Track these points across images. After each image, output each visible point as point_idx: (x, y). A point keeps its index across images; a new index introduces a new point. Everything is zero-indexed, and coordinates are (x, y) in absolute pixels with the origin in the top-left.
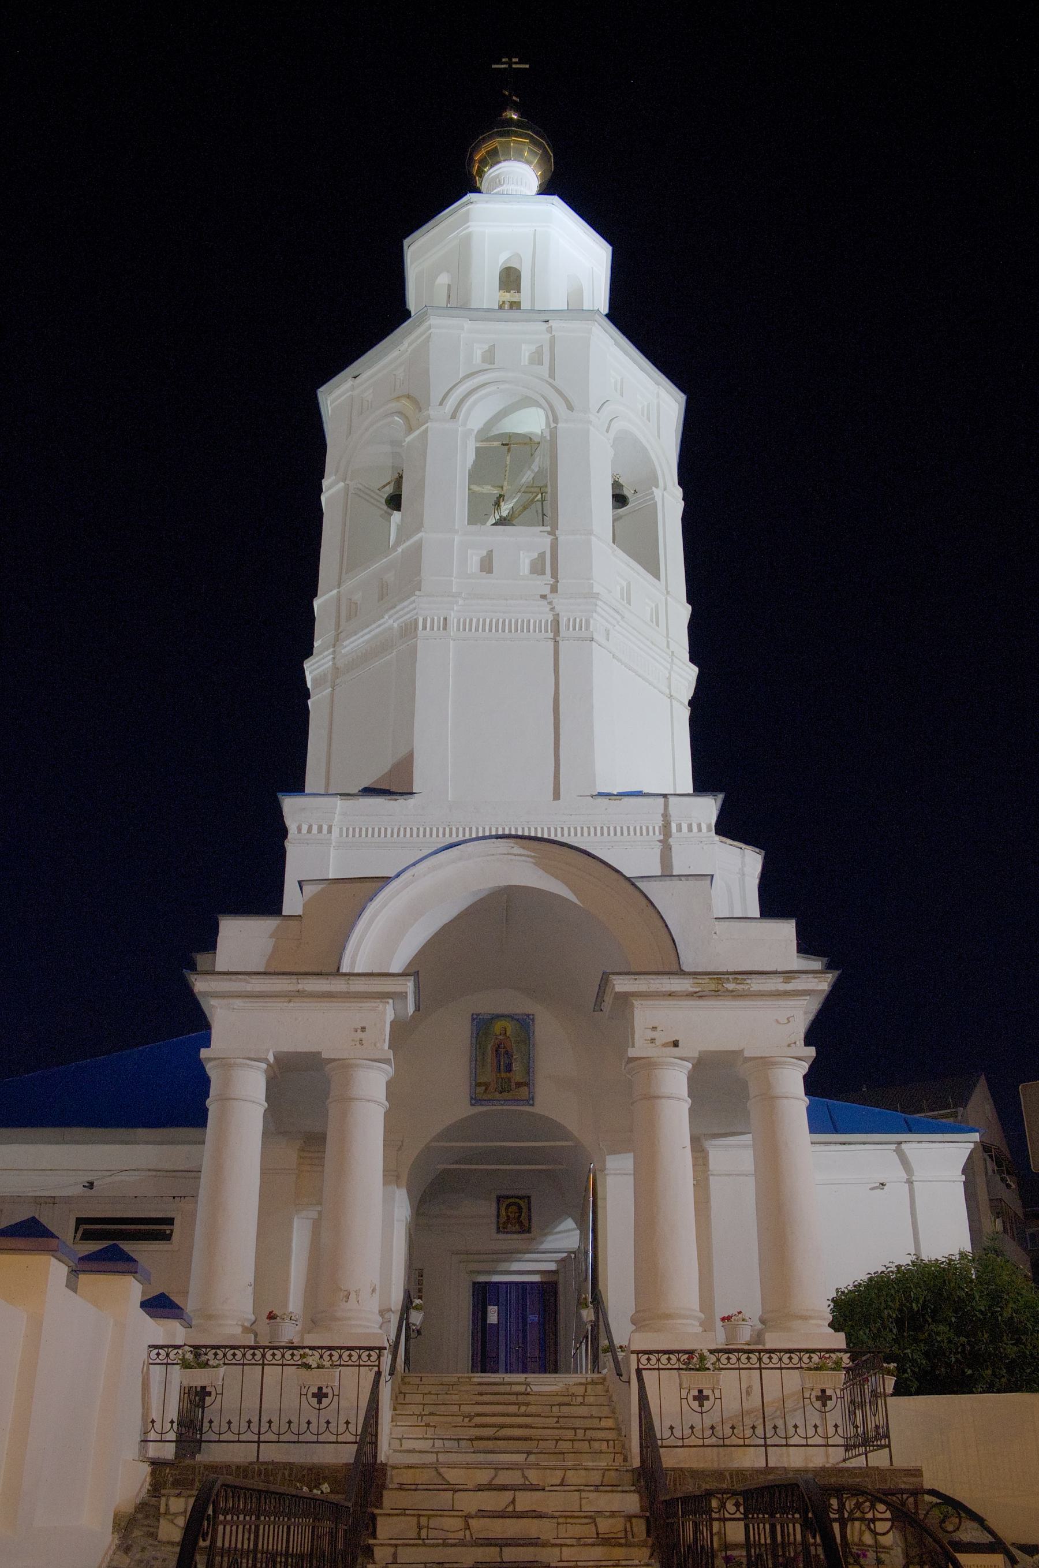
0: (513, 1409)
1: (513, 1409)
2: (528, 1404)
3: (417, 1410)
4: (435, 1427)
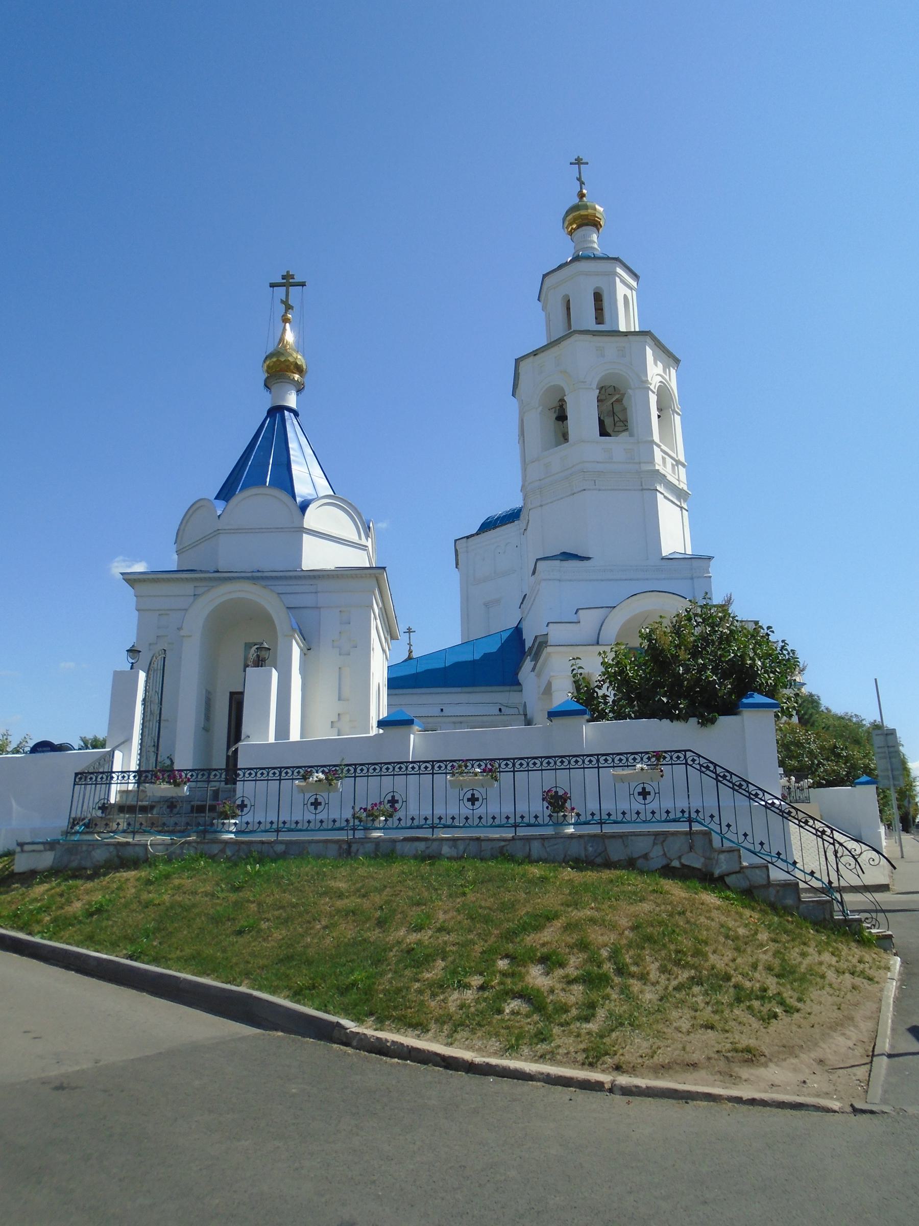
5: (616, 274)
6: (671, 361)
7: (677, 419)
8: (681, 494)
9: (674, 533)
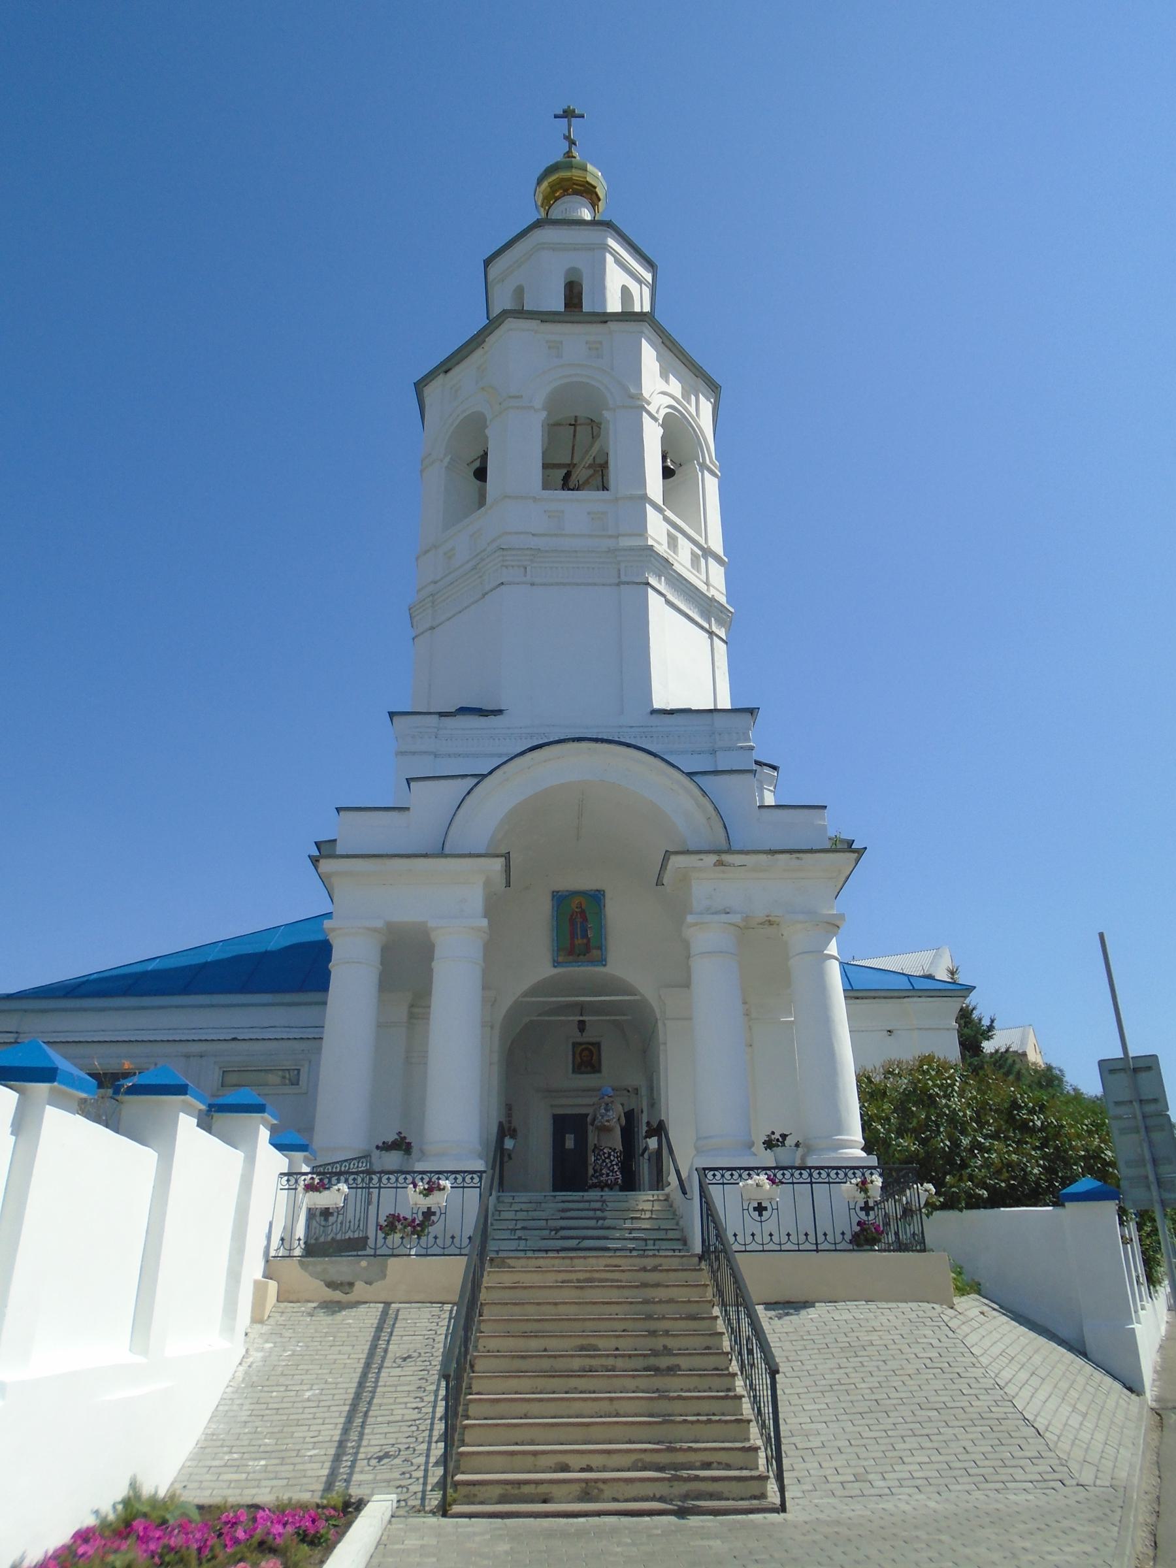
0: (592, 1223)
1: (592, 1223)
2: (604, 1219)
3: (511, 1225)
5: (606, 248)
6: (700, 383)
7: (711, 485)
8: (707, 606)
9: (686, 667)
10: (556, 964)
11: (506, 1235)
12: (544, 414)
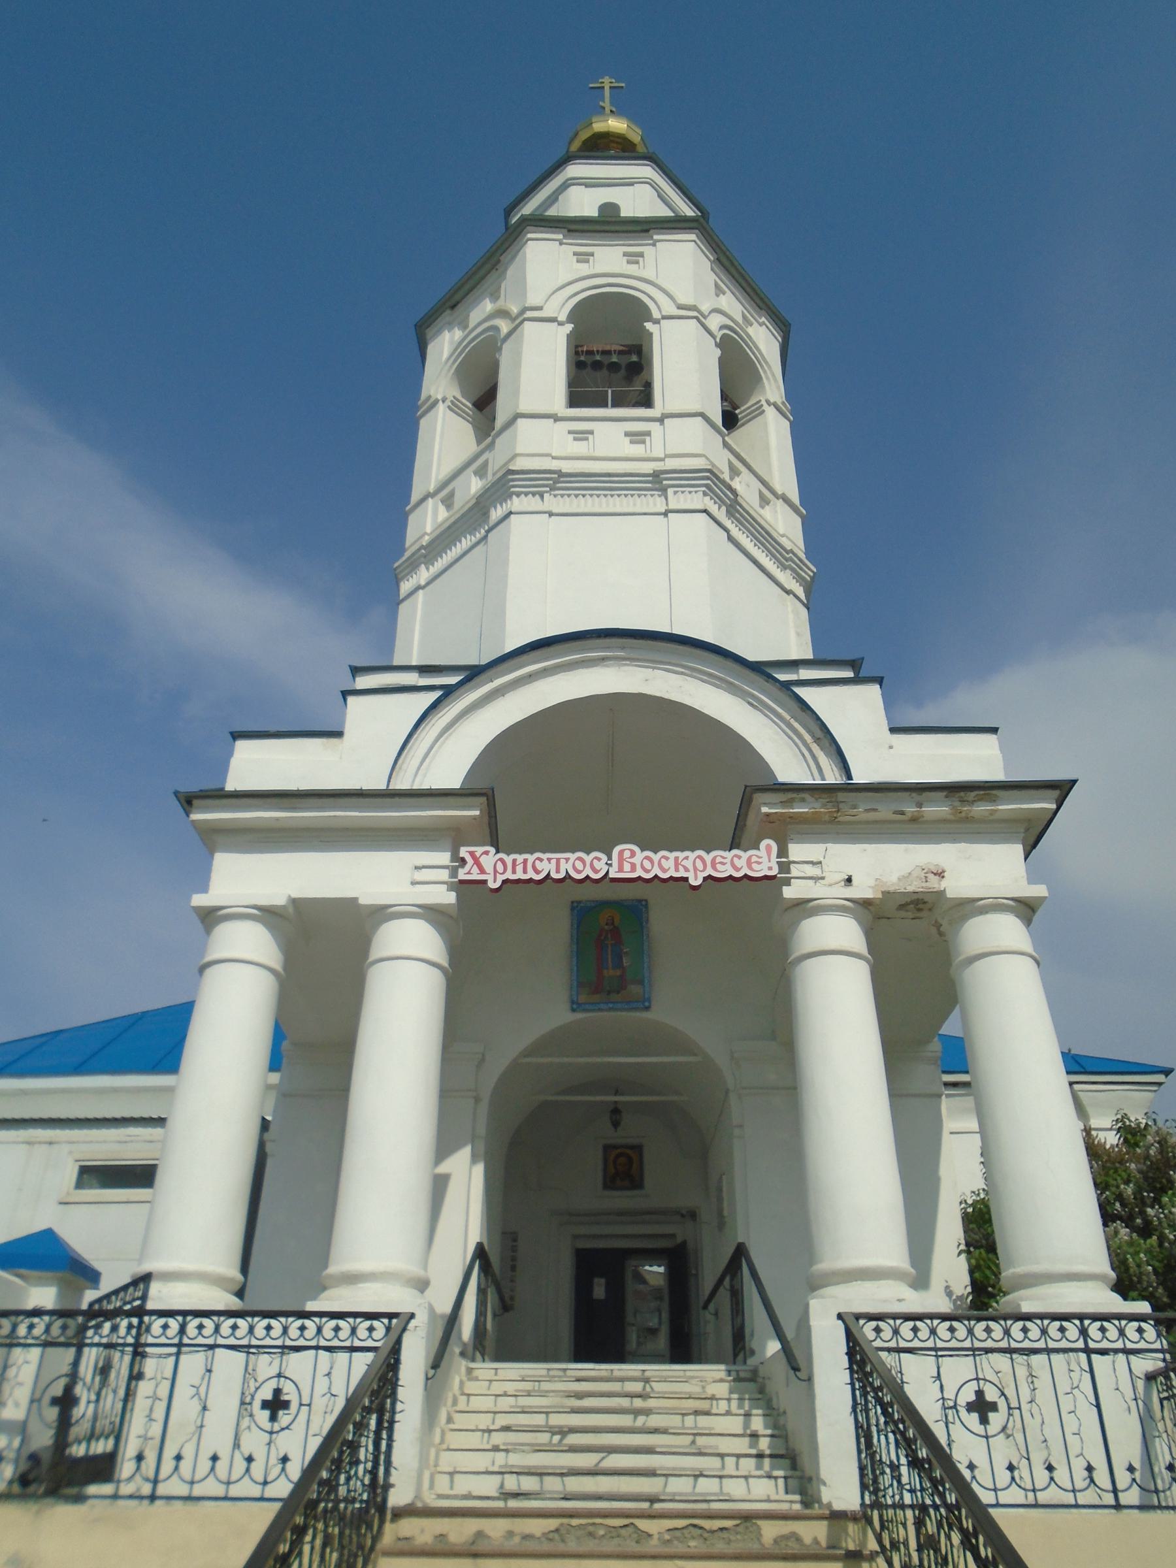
0: (625, 1420)
1: (625, 1420)
2: (647, 1412)
3: (484, 1421)
4: (507, 1451)
10: (575, 1006)
11: (475, 1440)
12: (569, 327)
